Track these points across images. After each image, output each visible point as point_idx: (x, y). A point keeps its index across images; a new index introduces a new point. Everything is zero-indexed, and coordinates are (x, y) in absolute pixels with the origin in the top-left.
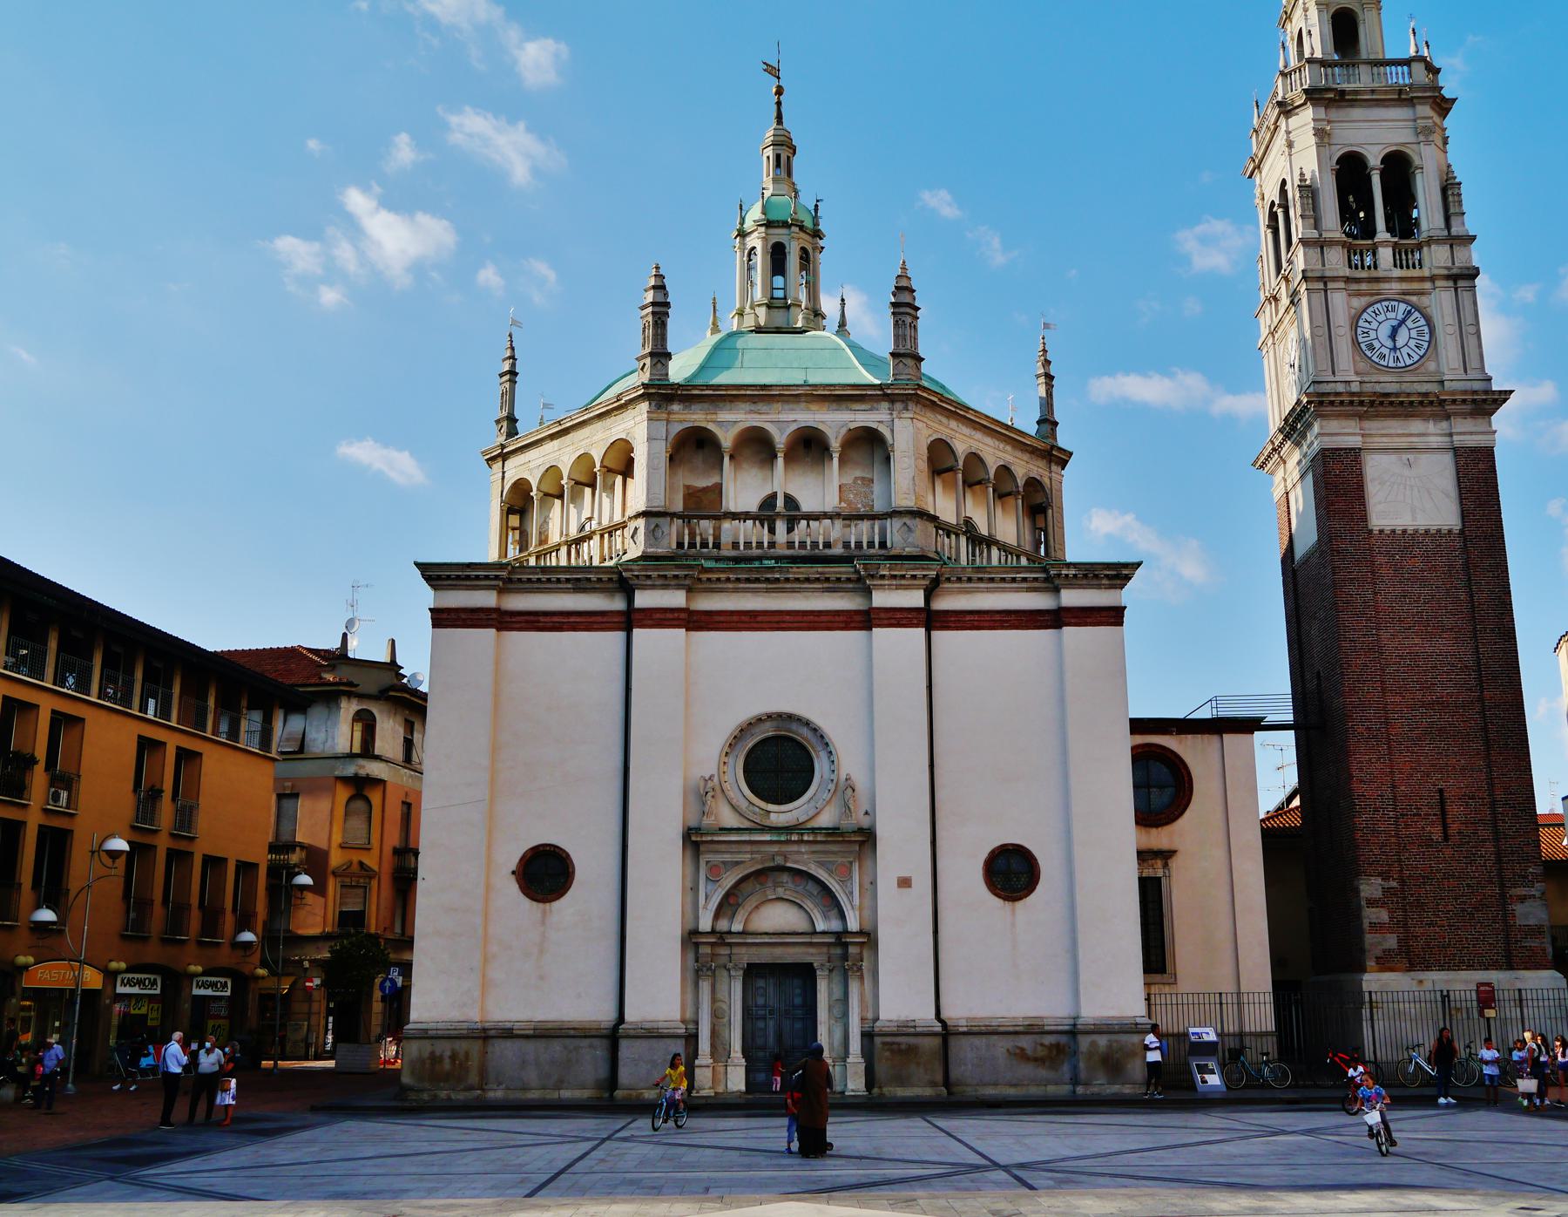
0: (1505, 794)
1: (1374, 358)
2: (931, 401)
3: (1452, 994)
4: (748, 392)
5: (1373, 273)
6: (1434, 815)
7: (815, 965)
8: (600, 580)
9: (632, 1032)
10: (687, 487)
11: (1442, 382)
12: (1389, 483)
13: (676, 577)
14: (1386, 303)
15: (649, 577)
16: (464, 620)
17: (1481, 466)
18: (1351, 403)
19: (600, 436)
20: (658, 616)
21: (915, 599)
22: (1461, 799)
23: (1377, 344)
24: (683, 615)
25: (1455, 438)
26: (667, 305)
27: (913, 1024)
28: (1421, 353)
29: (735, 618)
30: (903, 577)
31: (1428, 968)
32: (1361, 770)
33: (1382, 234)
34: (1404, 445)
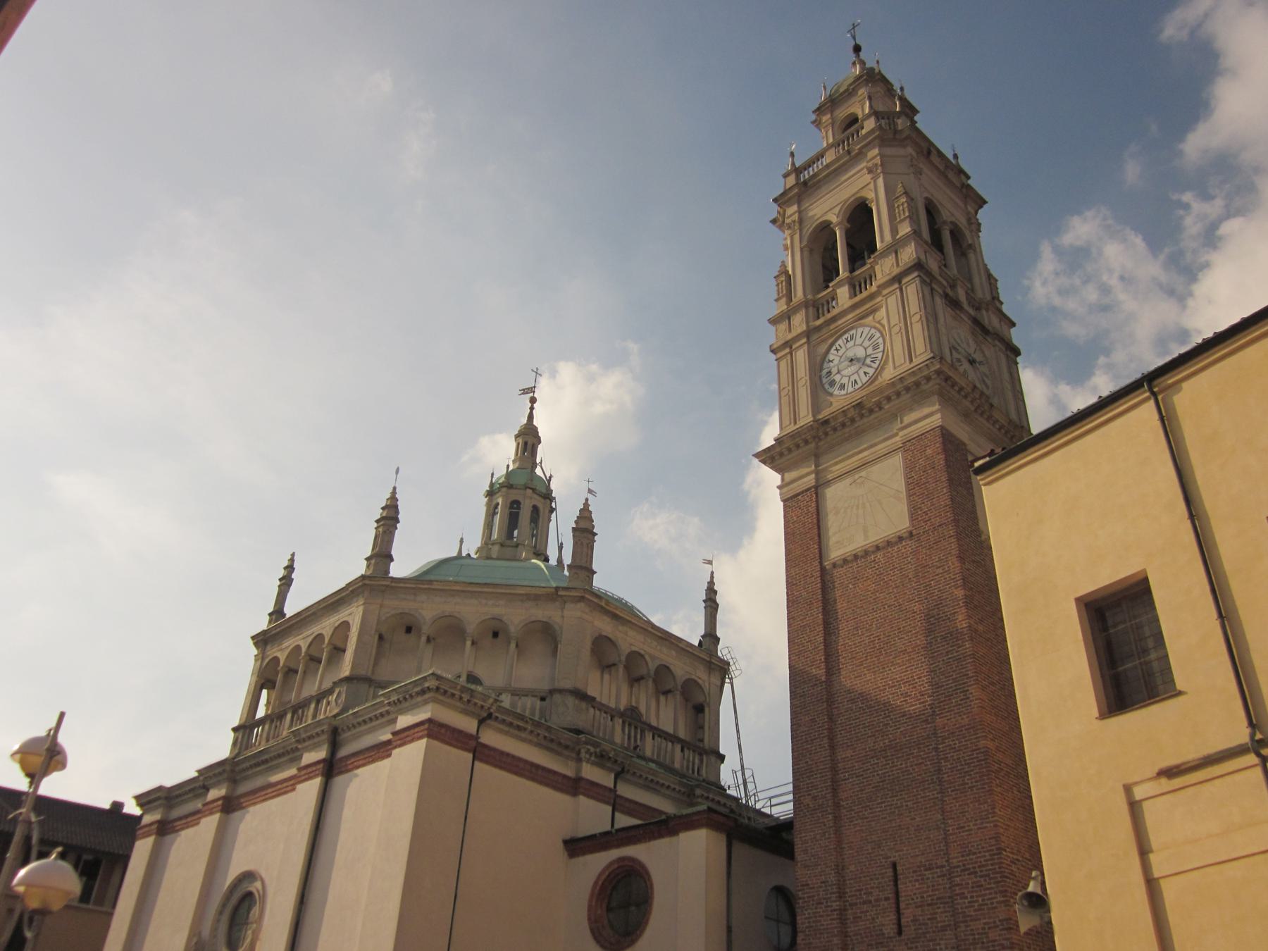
0: (963, 856)
2: (387, 586)
6: (887, 899)
17: (929, 451)
22: (914, 872)
32: (805, 851)
34: (856, 465)
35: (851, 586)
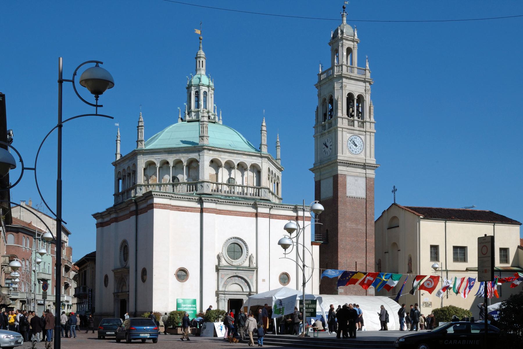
1: (351, 151)
4: (230, 151)
7: (244, 299)
8: (195, 199)
10: (210, 174)
11: (365, 160)
12: (352, 185)
13: (215, 200)
14: (354, 136)
15: (208, 200)
16: (162, 207)
17: (371, 183)
18: (346, 163)
19: (184, 155)
20: (209, 210)
21: (266, 210)
24: (215, 210)
25: (367, 174)
29: (226, 212)
30: (266, 205)
35: (352, 204)
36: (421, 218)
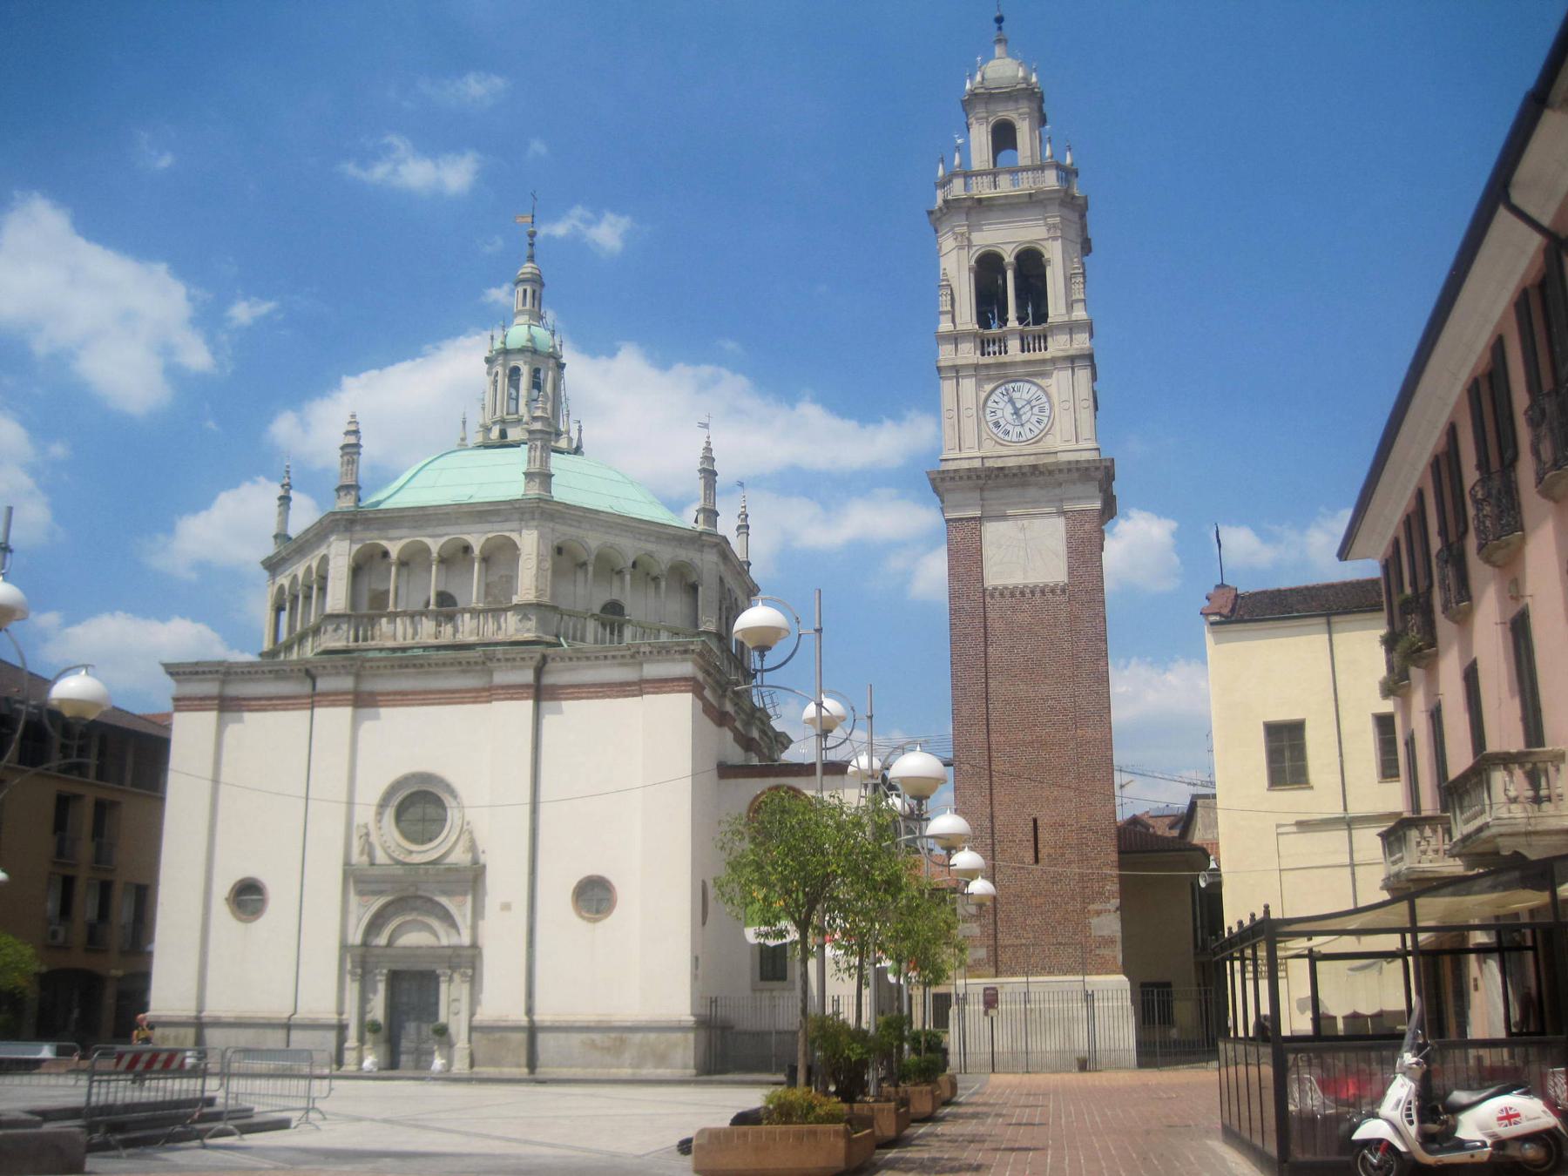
1: (1000, 435)
3: (1095, 993)
4: (411, 513)
5: (1003, 358)
9: (299, 1022)
13: (343, 666)
14: (1013, 384)
15: (324, 667)
17: (1087, 527)
23: (1002, 422)
26: (357, 446)
27: (504, 1018)
28: (1041, 427)
30: (514, 659)
31: (1013, 974)
33: (1013, 323)
36: (1212, 624)
